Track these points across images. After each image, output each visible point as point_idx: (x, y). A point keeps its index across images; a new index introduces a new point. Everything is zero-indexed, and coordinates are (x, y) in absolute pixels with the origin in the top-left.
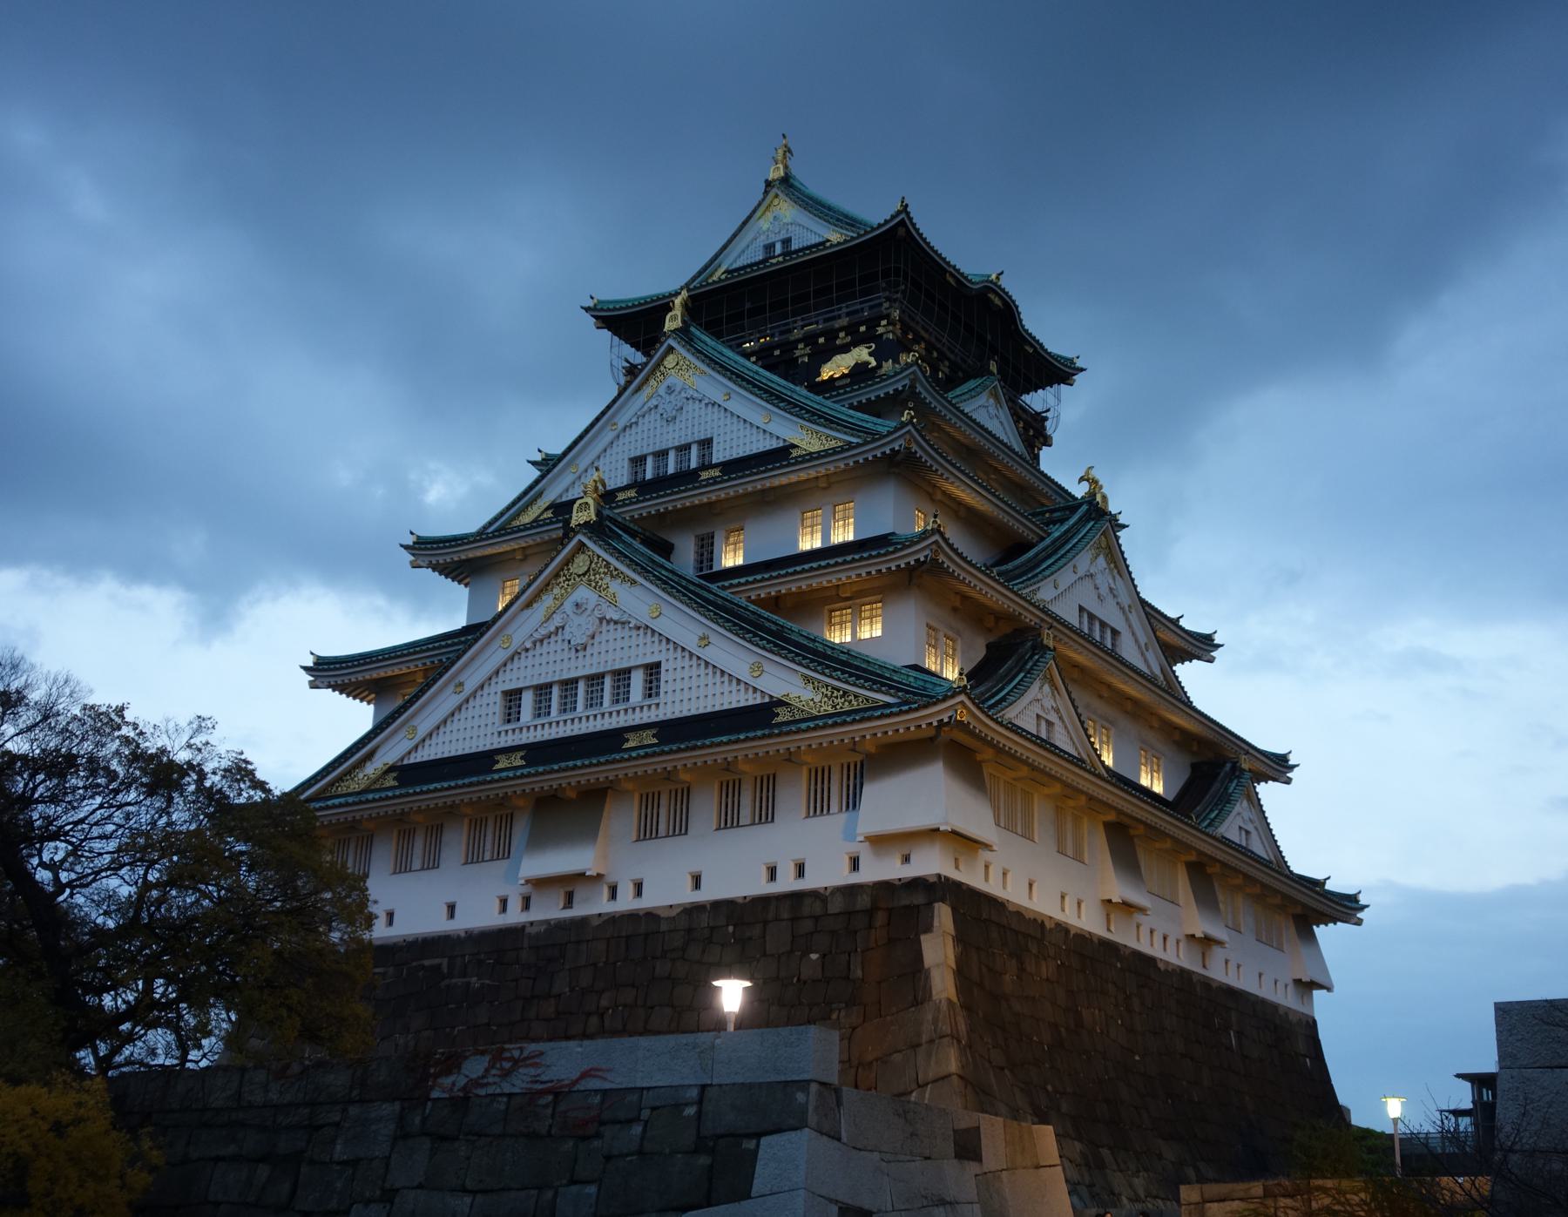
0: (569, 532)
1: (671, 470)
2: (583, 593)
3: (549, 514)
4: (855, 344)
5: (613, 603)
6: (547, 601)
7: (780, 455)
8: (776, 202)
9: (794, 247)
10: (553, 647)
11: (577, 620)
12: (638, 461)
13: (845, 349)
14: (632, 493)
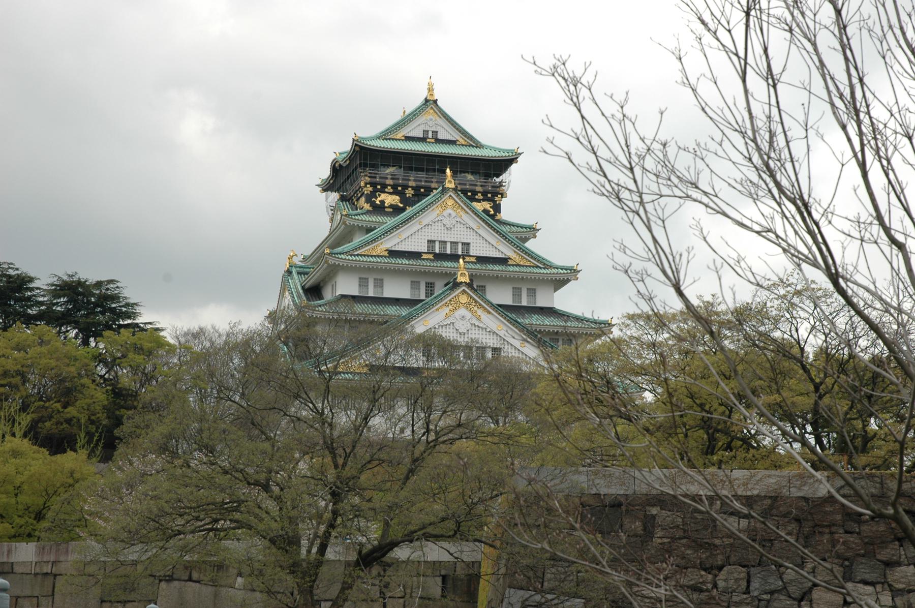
0: (456, 285)
1: (448, 252)
2: (462, 311)
3: (386, 254)
4: (484, 200)
5: (479, 318)
6: (446, 310)
7: (503, 261)
8: (431, 111)
9: (440, 137)
10: (448, 330)
11: (462, 322)
12: (431, 242)
13: (479, 201)
14: (431, 257)
